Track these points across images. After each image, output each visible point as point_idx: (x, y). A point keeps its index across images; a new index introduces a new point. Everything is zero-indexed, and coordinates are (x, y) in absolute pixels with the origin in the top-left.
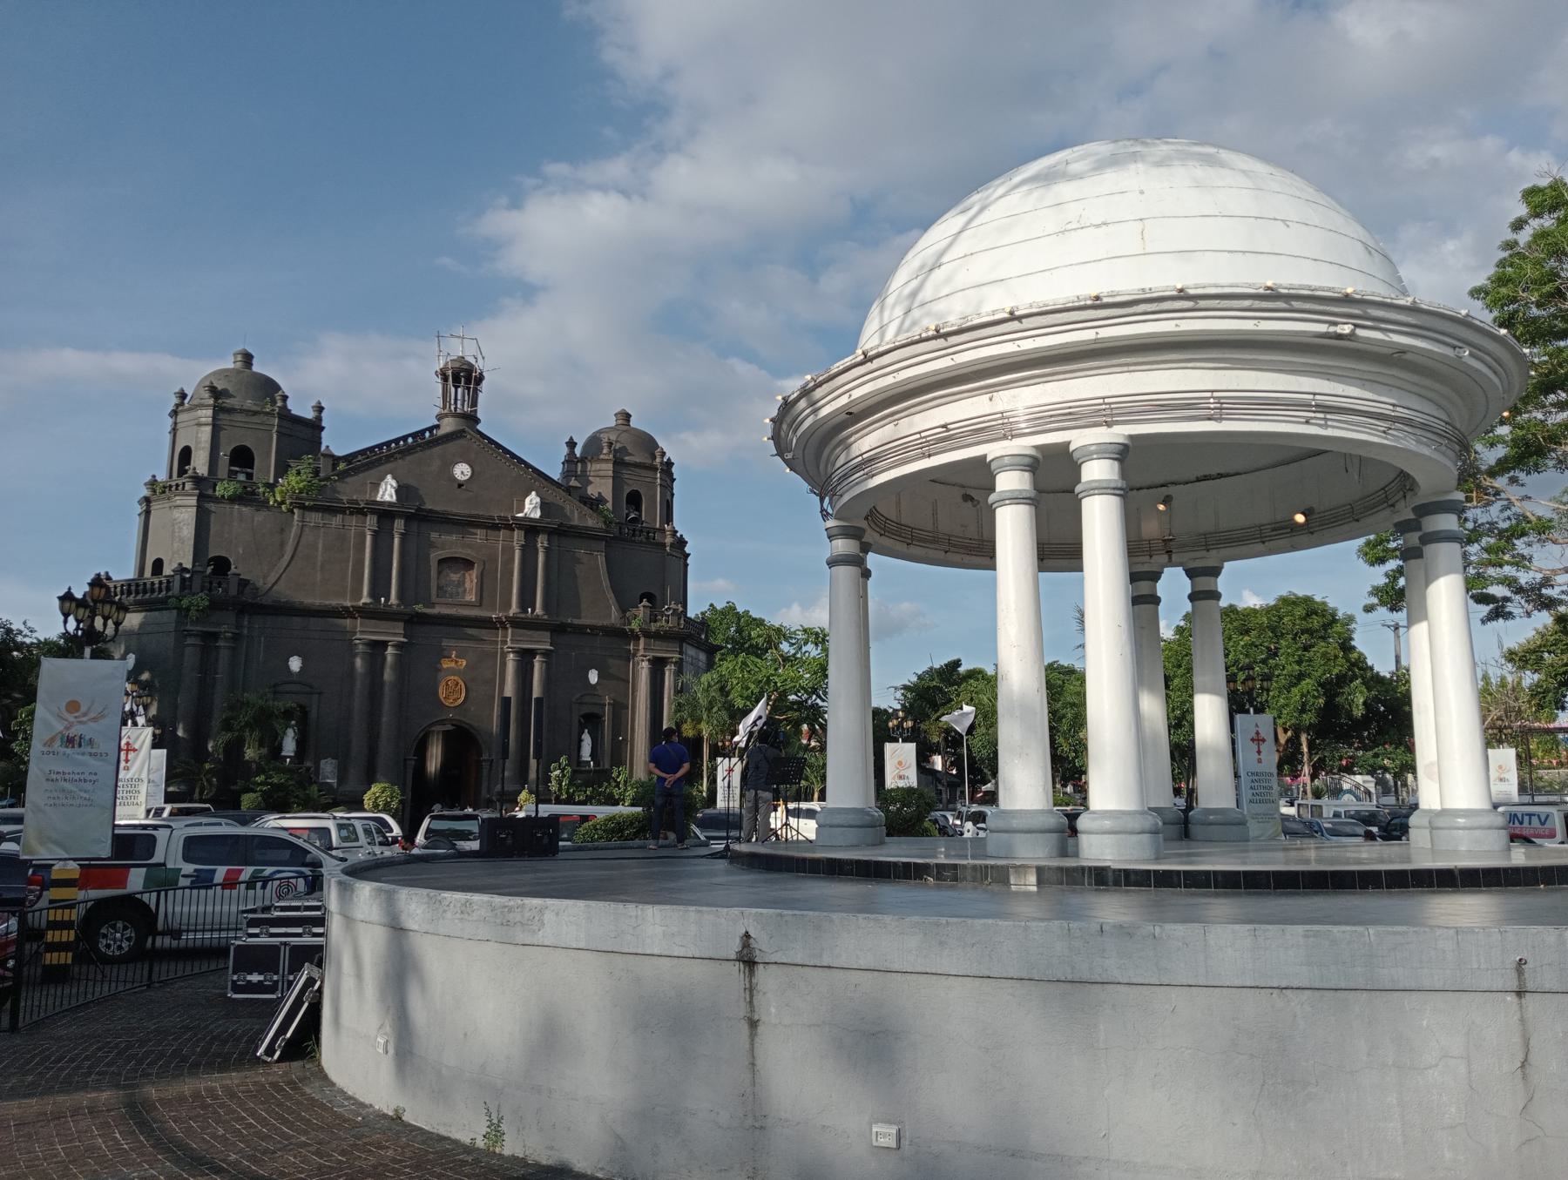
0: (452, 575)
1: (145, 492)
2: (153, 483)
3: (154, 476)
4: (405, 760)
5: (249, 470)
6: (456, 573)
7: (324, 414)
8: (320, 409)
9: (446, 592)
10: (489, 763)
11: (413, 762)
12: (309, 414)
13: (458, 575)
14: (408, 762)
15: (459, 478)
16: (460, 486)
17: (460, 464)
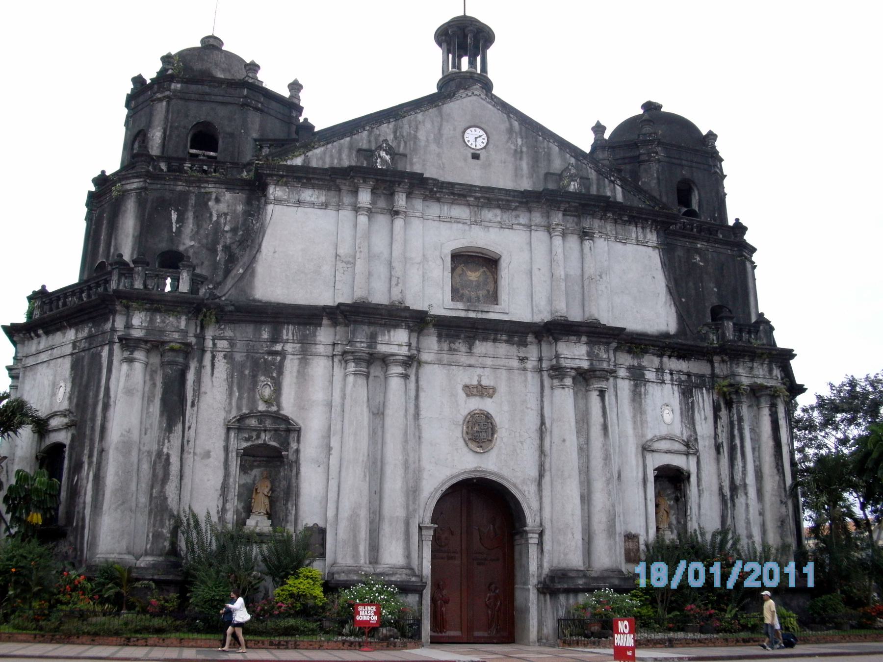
0: (469, 273)
1: (93, 188)
2: (102, 181)
3: (103, 172)
4: (420, 528)
5: (212, 154)
6: (476, 271)
7: (302, 94)
8: (295, 87)
9: (462, 294)
10: (537, 536)
11: (432, 532)
12: (286, 93)
13: (478, 274)
14: (424, 532)
15: (473, 147)
16: (476, 156)
17: (473, 129)
